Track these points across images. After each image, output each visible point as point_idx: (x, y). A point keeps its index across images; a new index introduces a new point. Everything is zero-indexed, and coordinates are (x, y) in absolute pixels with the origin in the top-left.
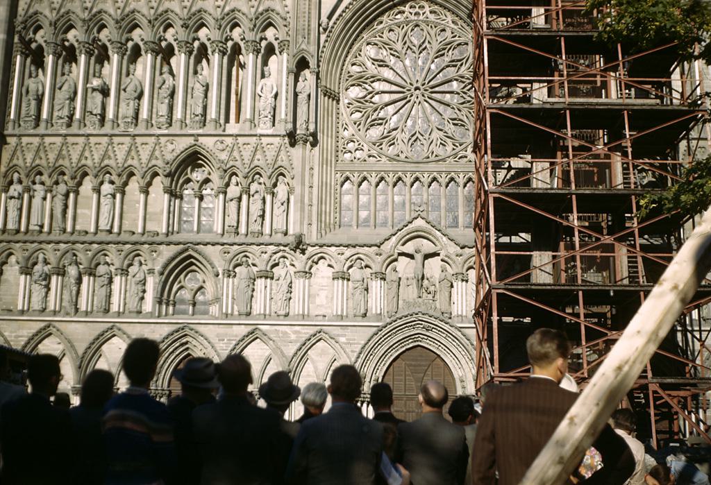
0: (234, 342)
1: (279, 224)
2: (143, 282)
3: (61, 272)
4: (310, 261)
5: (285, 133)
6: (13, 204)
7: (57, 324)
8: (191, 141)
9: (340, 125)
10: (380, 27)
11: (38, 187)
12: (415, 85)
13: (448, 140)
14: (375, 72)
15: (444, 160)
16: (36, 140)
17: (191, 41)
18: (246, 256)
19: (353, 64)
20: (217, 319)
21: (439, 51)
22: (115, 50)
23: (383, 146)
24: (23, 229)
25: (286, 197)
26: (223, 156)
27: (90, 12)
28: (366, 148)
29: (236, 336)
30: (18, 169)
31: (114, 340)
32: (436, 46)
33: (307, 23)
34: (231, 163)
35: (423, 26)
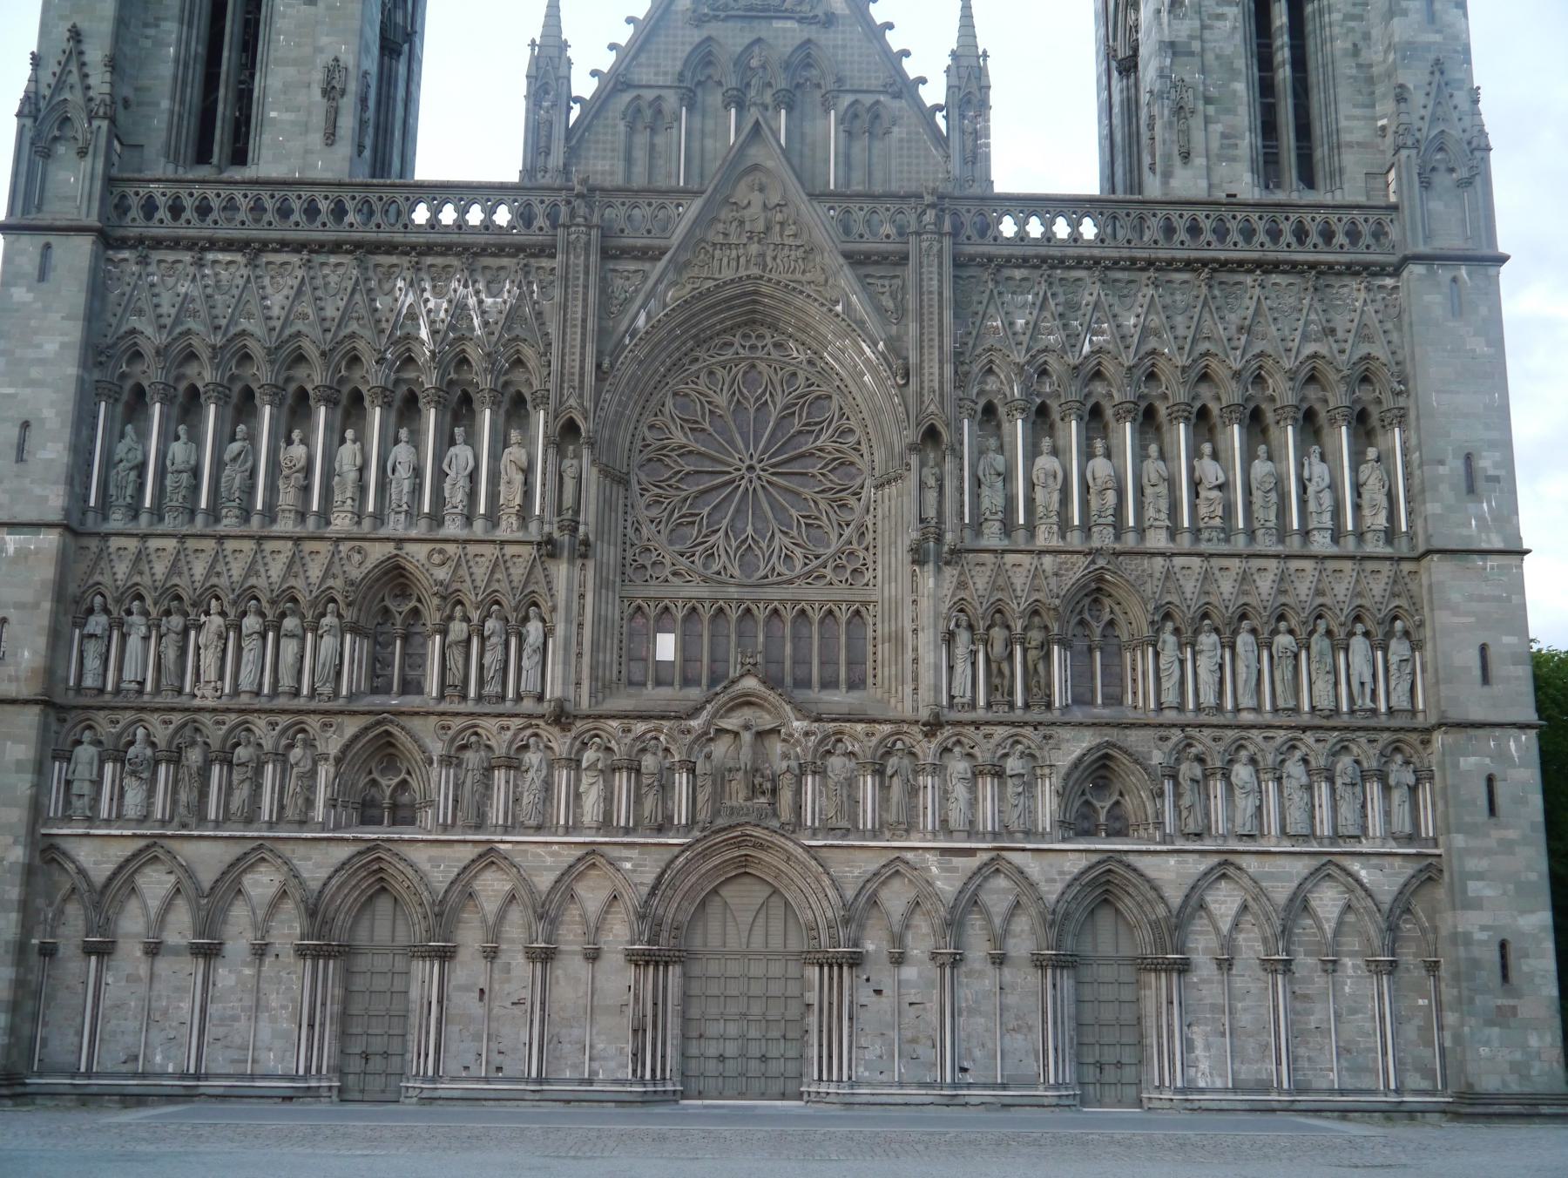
0: (456, 871)
1: (530, 683)
2: (313, 773)
3: (175, 757)
4: (578, 743)
5: (539, 539)
6: (92, 648)
7: (169, 844)
8: (390, 548)
9: (629, 524)
10: (694, 367)
11: (136, 618)
12: (748, 462)
13: (798, 551)
14: (684, 441)
15: (791, 582)
16: (132, 544)
17: (390, 386)
18: (476, 734)
19: (651, 427)
20: (430, 832)
21: (787, 407)
22: (267, 398)
23: (696, 558)
24: (109, 687)
25: (541, 640)
26: (442, 574)
27: (224, 334)
28: (667, 561)
29: (459, 860)
30: (103, 589)
31: (262, 868)
32: (781, 401)
33: (577, 364)
34: (455, 586)
35: (762, 366)
